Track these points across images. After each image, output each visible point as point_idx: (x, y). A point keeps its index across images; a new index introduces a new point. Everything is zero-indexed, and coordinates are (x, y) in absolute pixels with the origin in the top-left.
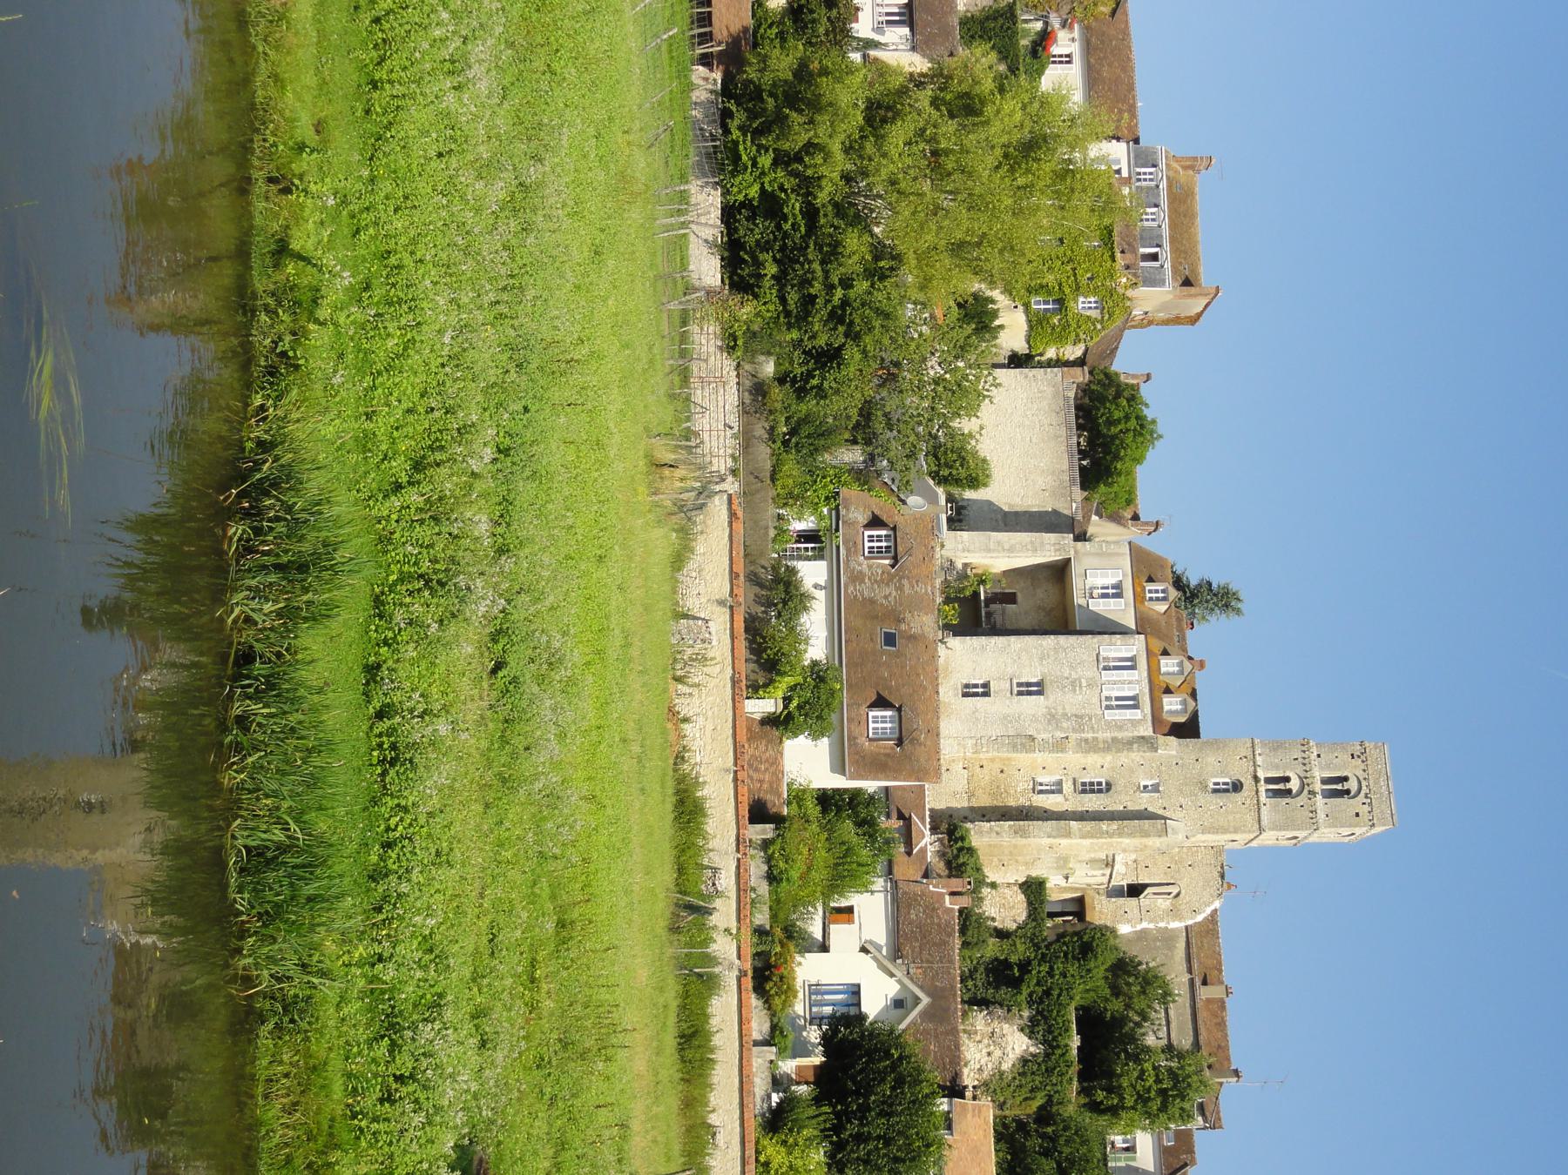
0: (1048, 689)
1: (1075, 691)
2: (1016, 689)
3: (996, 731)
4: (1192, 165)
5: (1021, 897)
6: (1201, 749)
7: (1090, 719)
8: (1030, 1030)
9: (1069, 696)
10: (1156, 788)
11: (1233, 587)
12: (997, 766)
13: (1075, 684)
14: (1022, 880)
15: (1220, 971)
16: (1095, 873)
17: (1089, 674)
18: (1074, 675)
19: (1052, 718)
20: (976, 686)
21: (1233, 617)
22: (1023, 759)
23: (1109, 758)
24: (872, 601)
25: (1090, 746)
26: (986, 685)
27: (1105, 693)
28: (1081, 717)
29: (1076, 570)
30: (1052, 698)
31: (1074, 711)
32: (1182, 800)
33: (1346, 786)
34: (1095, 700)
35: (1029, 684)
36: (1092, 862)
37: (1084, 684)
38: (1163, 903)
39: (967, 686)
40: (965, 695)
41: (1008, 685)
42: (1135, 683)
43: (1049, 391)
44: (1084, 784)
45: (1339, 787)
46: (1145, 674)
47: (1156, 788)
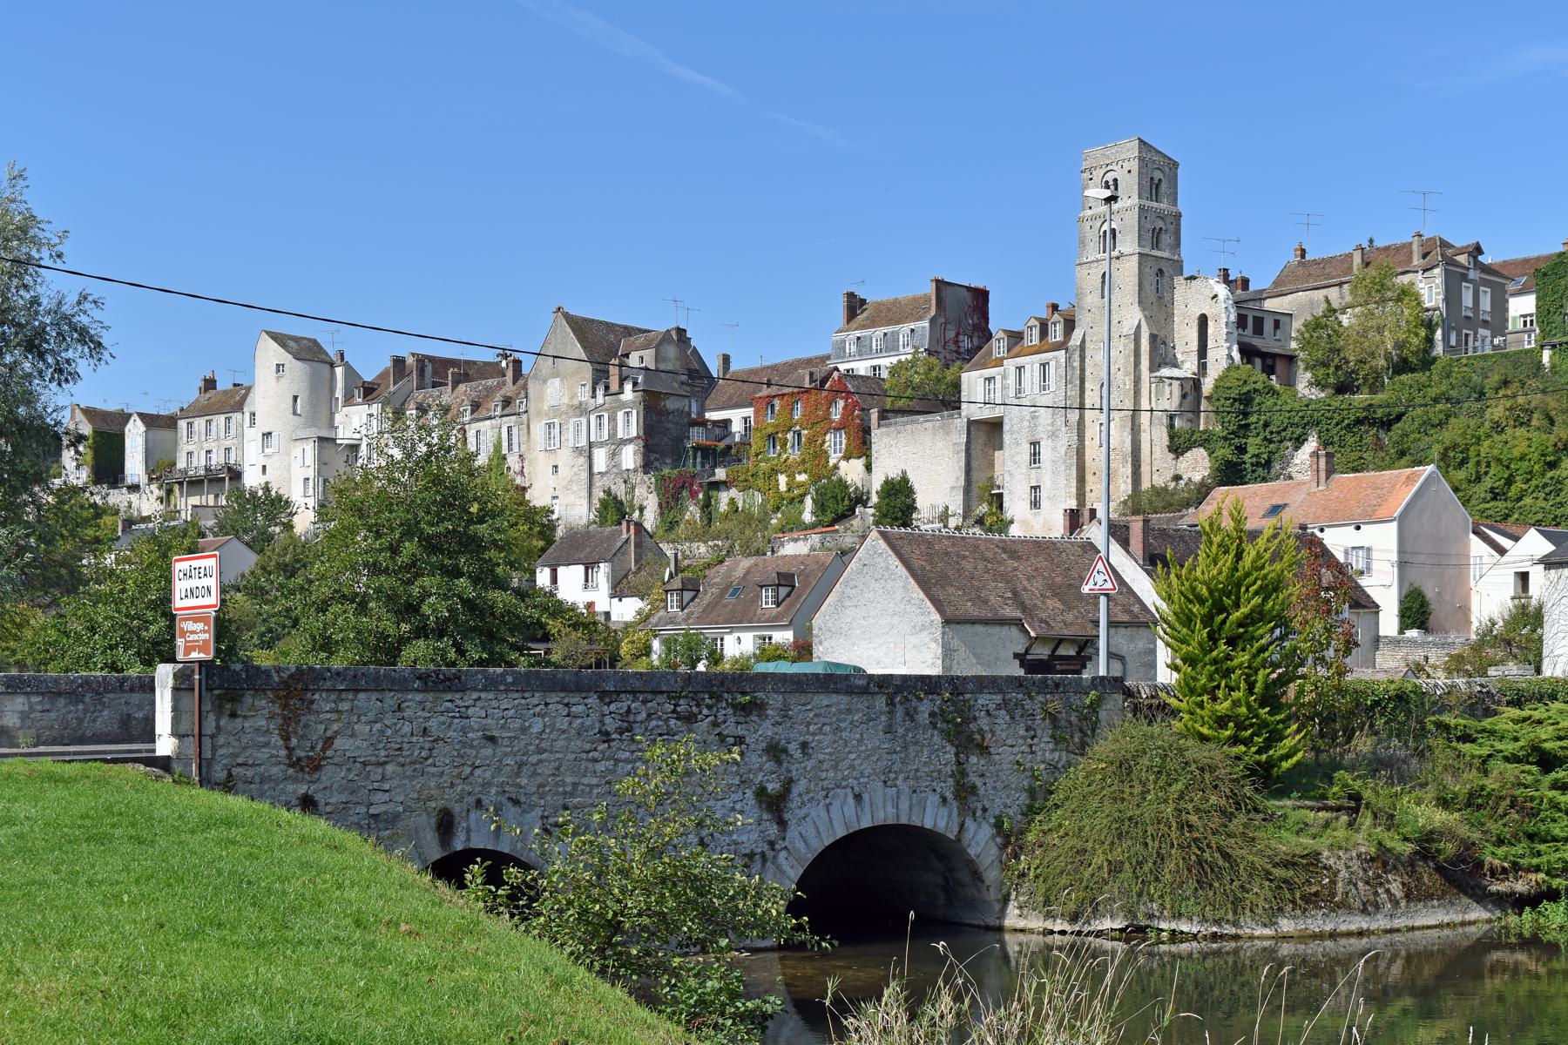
5: (1188, 454)
6: (1082, 308)
8: (1299, 442)
19: (1053, 435)
33: (1111, 183)
41: (1033, 471)
43: (886, 440)
46: (1028, 358)
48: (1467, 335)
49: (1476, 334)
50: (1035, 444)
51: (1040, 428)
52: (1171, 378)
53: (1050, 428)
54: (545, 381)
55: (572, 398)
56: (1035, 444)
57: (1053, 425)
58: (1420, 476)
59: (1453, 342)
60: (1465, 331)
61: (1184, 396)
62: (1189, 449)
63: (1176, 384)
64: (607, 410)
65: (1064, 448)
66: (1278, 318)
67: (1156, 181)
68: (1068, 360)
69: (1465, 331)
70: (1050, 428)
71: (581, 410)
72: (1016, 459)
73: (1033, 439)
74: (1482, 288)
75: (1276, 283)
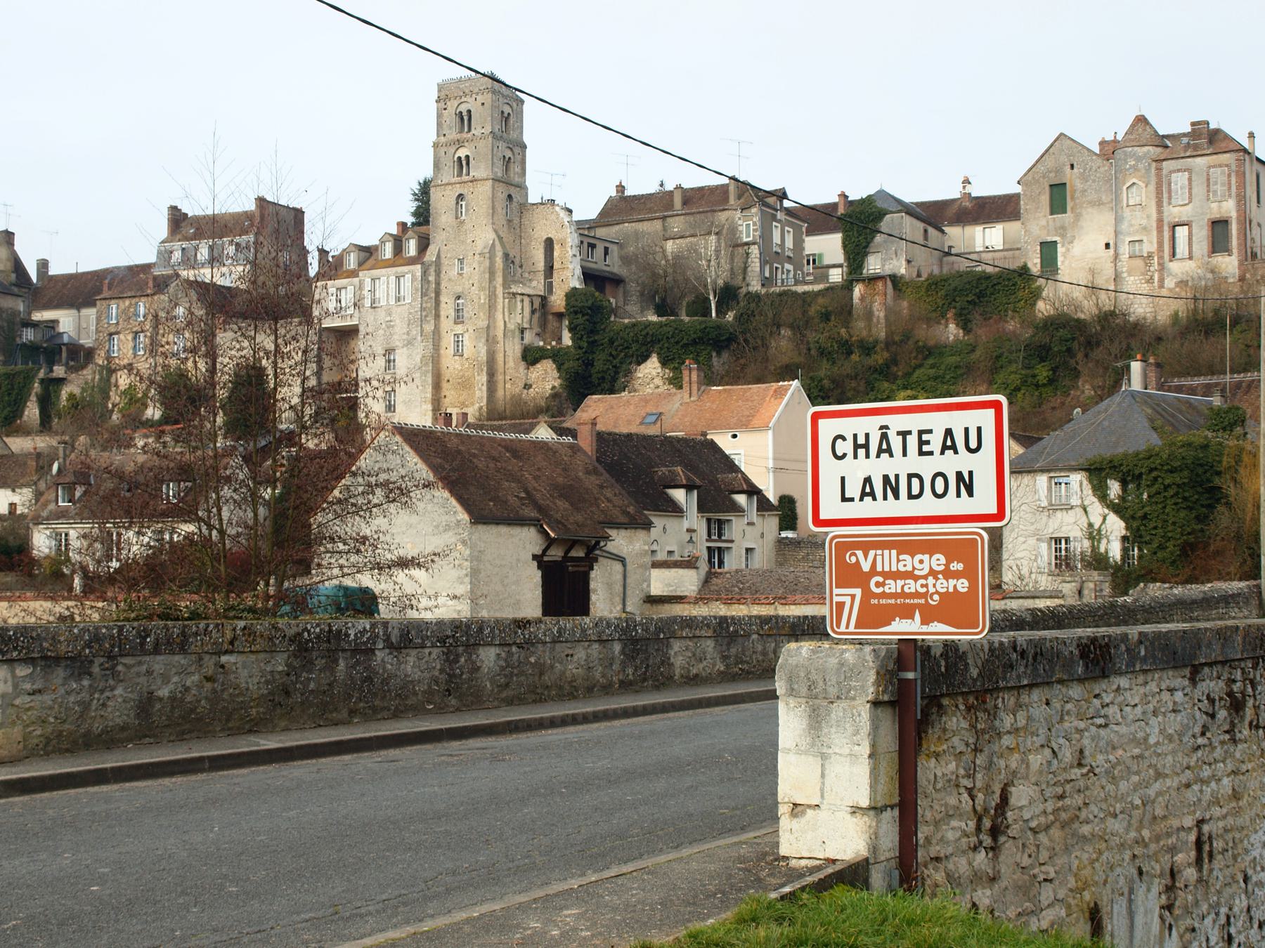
0: (392, 345)
1: (393, 326)
4: (177, 219)
5: (538, 366)
7: (410, 313)
9: (397, 329)
10: (461, 261)
14: (523, 365)
16: (519, 305)
28: (409, 320)
30: (398, 343)
31: (405, 326)
32: (469, 241)
33: (465, 113)
34: (399, 309)
37: (388, 319)
45: (466, 118)
46: (384, 271)
47: (461, 261)
48: (777, 268)
49: (783, 268)
51: (395, 337)
52: (523, 294)
53: (405, 337)
57: (408, 334)
58: (787, 390)
59: (767, 275)
60: (775, 265)
61: (533, 312)
63: (527, 300)
65: (420, 356)
66: (607, 245)
67: (506, 115)
68: (425, 273)
69: (775, 265)
70: (405, 337)
73: (388, 346)
74: (787, 228)
75: (602, 214)
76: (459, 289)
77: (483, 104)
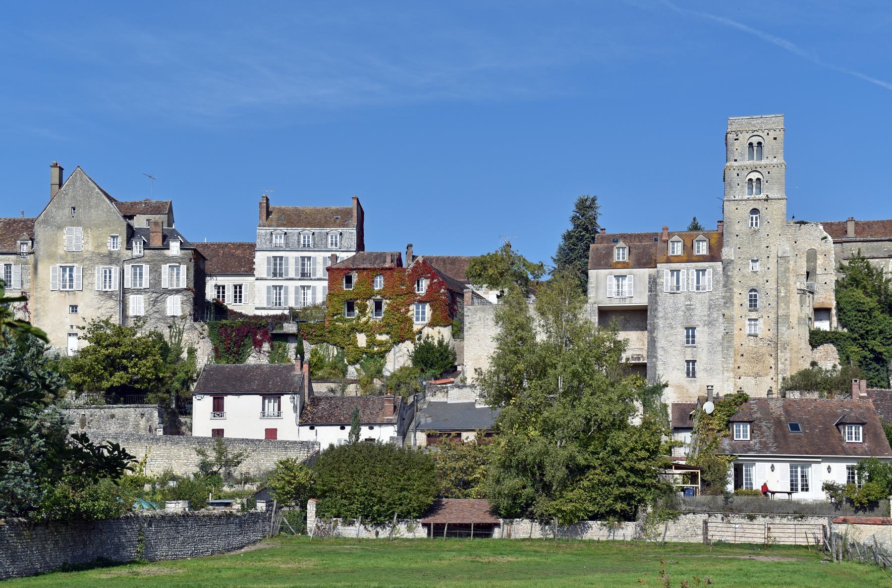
0: (693, 324)
1: (693, 309)
2: (690, 345)
3: (719, 357)
5: (821, 348)
9: (697, 312)
11: (575, 200)
12: (739, 358)
13: (689, 308)
15: (832, 224)
17: (683, 299)
18: (683, 308)
19: (710, 324)
20: (688, 369)
21: (598, 203)
22: (736, 342)
23: (735, 290)
24: (775, 437)
25: (728, 301)
26: (688, 362)
27: (695, 290)
28: (710, 306)
29: (607, 303)
32: (764, 246)
34: (699, 296)
35: (688, 337)
36: (802, 303)
37: (689, 303)
38: (820, 261)
39: (688, 374)
40: (694, 376)
41: (689, 349)
42: (688, 271)
43: (480, 314)
44: (751, 306)
46: (683, 264)
50: (690, 330)
53: (706, 318)
54: (60, 227)
55: (98, 247)
56: (690, 330)
57: (709, 316)
62: (822, 343)
64: (146, 262)
65: (722, 334)
70: (706, 318)
71: (111, 258)
72: (671, 338)
73: (688, 325)
76: (753, 284)
77: (775, 139)
